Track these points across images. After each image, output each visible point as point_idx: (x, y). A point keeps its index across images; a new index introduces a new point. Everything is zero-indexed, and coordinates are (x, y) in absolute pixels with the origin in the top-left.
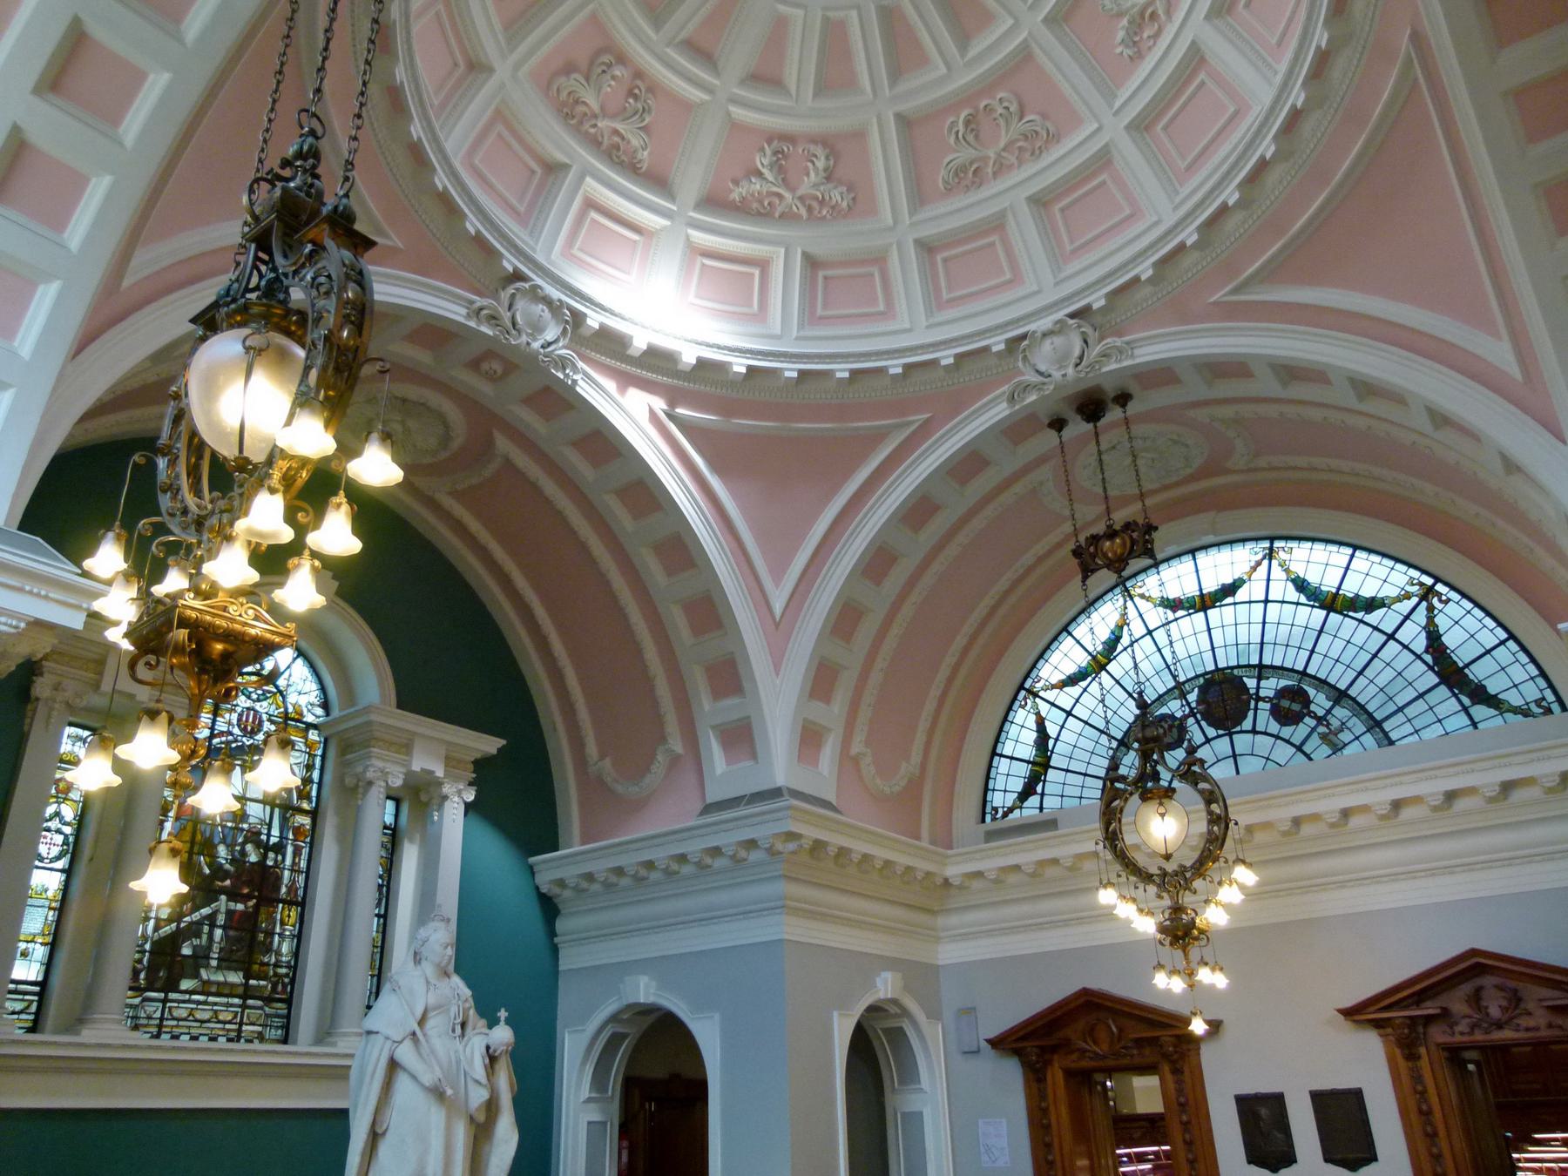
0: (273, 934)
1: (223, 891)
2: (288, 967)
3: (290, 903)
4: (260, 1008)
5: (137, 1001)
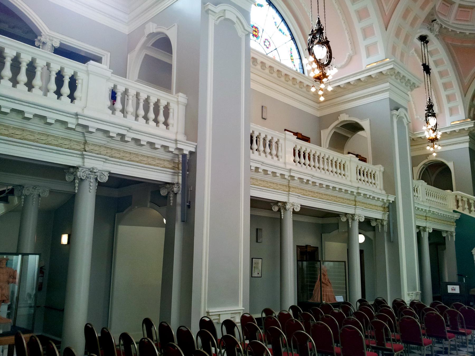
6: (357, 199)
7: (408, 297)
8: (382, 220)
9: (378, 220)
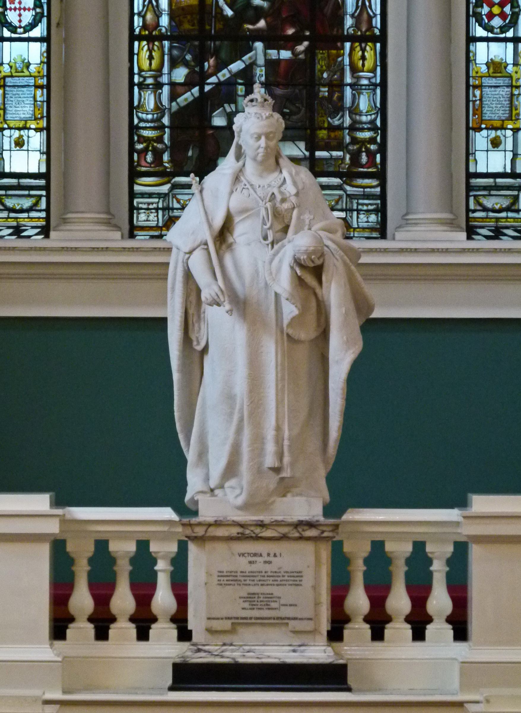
0: (341, 85)
1: (258, 36)
2: (374, 128)
3: (361, 39)
4: (339, 187)
5: (165, 189)
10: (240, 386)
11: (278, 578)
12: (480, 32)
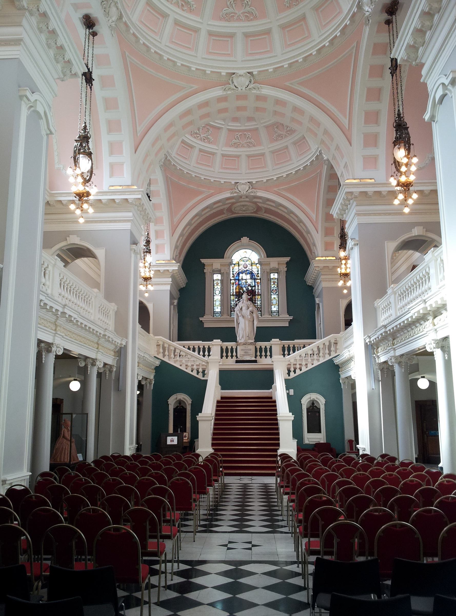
6: (100, 342)
7: (129, 450)
8: (111, 366)
9: (107, 366)
10: (243, 327)
11: (248, 350)
12: (272, 294)
